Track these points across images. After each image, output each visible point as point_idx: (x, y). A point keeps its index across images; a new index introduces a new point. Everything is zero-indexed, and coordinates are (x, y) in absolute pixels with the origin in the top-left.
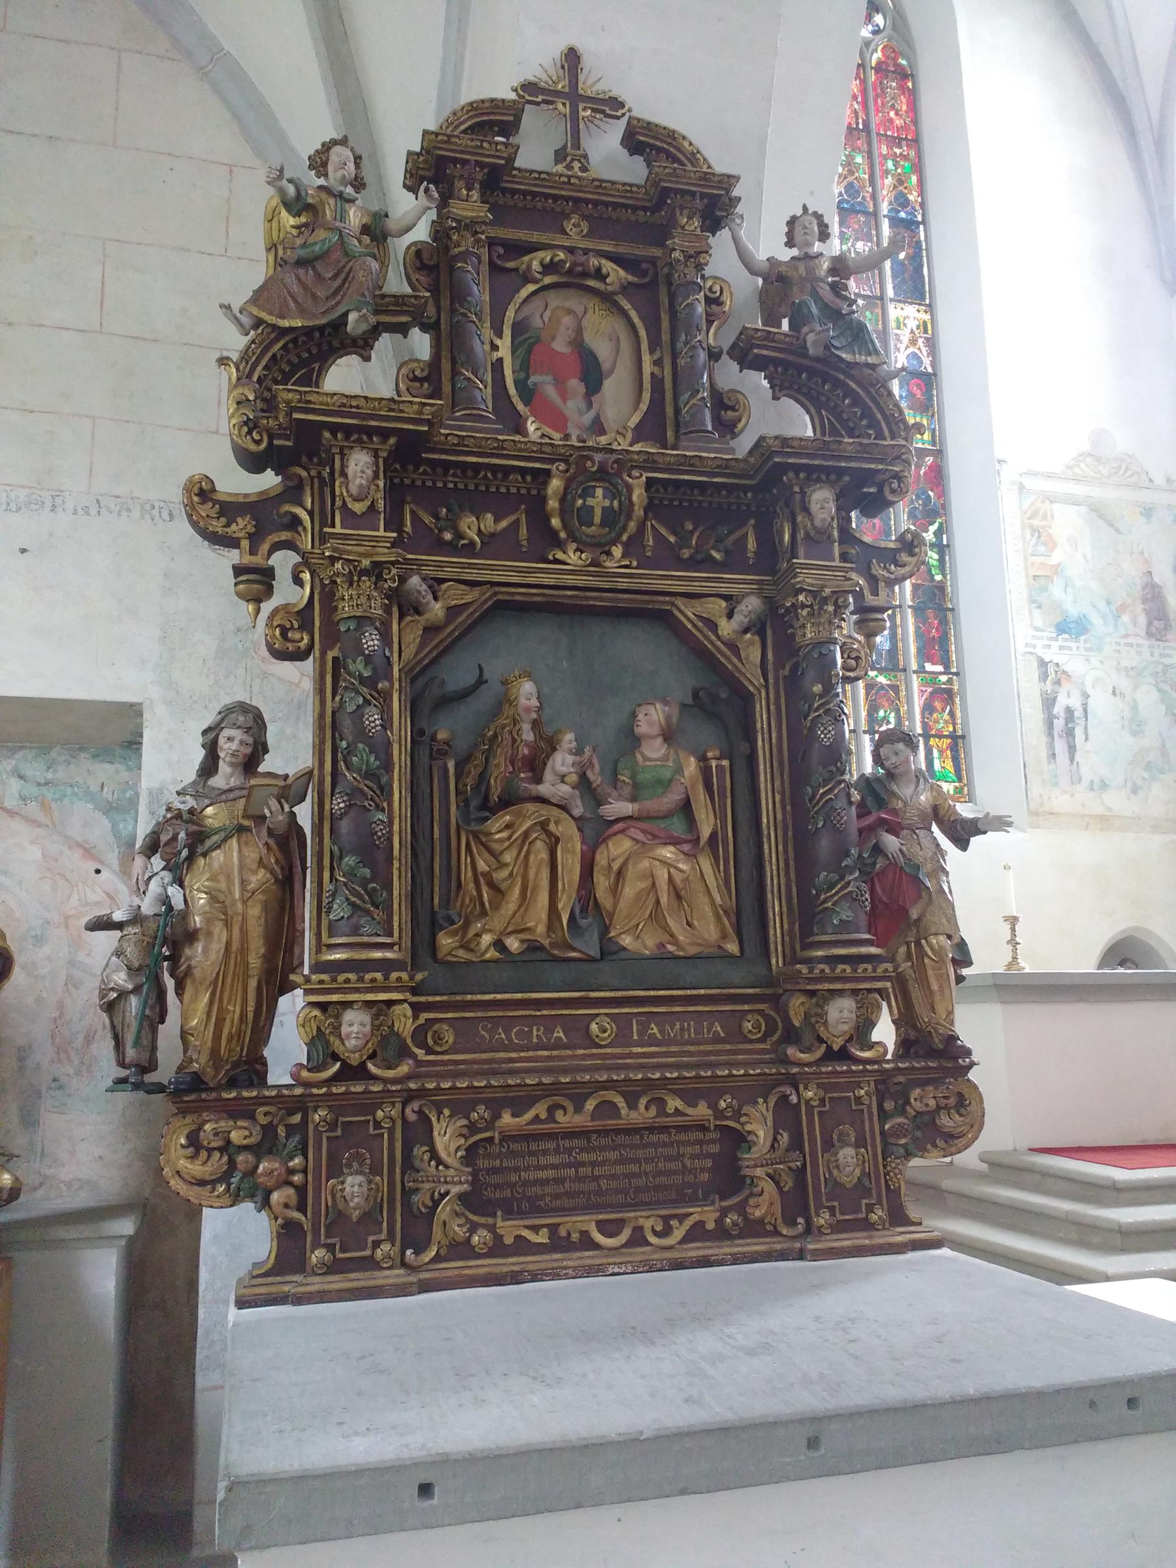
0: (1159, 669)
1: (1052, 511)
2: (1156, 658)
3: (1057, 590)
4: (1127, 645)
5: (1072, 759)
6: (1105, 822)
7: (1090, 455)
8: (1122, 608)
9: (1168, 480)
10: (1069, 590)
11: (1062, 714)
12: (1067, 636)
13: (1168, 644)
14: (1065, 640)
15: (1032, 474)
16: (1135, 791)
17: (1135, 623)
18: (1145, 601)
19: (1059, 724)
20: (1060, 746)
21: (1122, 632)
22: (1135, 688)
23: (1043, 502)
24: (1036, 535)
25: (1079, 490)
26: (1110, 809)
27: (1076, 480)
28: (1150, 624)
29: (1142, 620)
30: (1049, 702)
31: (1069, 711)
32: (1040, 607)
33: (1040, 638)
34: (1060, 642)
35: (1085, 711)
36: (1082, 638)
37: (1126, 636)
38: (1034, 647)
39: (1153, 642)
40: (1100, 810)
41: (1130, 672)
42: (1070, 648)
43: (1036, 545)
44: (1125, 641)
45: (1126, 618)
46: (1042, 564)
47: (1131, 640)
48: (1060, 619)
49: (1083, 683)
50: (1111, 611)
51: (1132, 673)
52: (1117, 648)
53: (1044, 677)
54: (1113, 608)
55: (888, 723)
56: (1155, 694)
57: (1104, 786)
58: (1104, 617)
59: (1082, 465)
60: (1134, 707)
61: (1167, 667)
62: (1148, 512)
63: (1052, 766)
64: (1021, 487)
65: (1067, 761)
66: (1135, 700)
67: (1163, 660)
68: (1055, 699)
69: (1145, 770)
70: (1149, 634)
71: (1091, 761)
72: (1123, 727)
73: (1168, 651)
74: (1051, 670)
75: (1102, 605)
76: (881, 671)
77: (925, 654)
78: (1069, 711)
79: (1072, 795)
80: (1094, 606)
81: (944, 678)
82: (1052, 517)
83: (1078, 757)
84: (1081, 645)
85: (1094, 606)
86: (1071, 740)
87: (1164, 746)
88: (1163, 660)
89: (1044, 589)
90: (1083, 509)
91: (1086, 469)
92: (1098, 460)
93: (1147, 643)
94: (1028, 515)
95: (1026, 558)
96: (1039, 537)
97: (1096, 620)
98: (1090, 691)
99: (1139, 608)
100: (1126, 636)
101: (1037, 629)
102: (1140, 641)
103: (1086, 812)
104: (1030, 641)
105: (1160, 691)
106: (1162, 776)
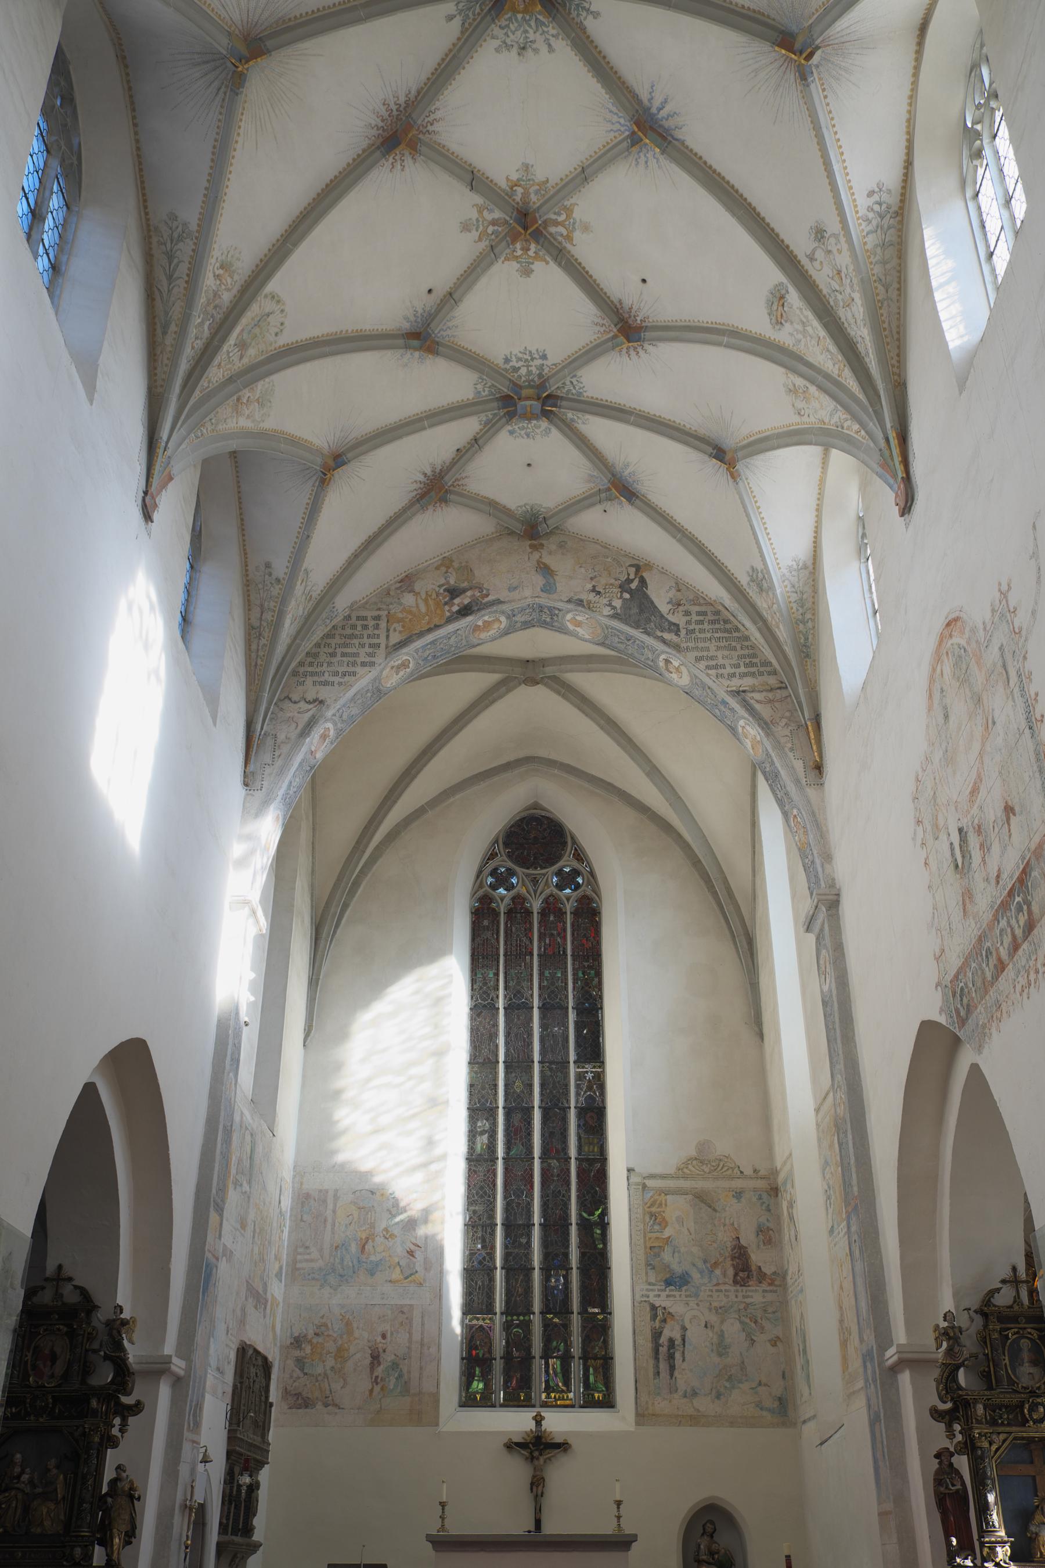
0: (742, 1306)
1: (666, 1201)
2: (740, 1299)
3: (667, 1256)
4: (717, 1291)
5: (672, 1375)
6: (695, 1420)
7: (696, 1159)
8: (716, 1264)
9: (755, 1171)
10: (676, 1254)
11: (666, 1343)
12: (673, 1288)
13: (749, 1288)
14: (671, 1290)
15: (652, 1176)
16: (718, 1396)
17: (724, 1275)
18: (733, 1258)
19: (663, 1350)
20: (663, 1366)
21: (715, 1281)
22: (722, 1322)
23: (660, 1195)
24: (653, 1218)
26: (698, 1411)
27: (685, 1177)
28: (736, 1275)
29: (731, 1272)
30: (657, 1335)
31: (671, 1341)
32: (654, 1268)
33: (652, 1290)
34: (667, 1293)
35: (684, 1340)
36: (685, 1288)
37: (718, 1284)
38: (648, 1297)
39: (738, 1287)
41: (722, 1311)
42: (674, 1296)
43: (652, 1226)
44: (716, 1288)
45: (718, 1272)
46: (657, 1238)
47: (722, 1287)
48: (668, 1276)
49: (683, 1320)
50: (707, 1268)
51: (720, 1311)
52: (710, 1293)
53: (654, 1317)
54: (708, 1265)
55: (559, 1350)
56: (737, 1326)
57: (695, 1394)
58: (701, 1272)
59: (690, 1167)
60: (721, 1335)
62: (738, 1195)
63: (657, 1380)
64: (644, 1186)
65: (669, 1377)
66: (722, 1331)
67: (746, 1300)
68: (661, 1333)
69: (727, 1381)
70: (735, 1282)
71: (685, 1376)
72: (712, 1350)
73: (750, 1294)
74: (660, 1312)
75: (700, 1264)
76: (556, 1315)
77: (585, 1302)
78: (671, 1341)
79: (670, 1401)
80: (694, 1265)
81: (600, 1317)
82: (666, 1205)
83: (676, 1373)
84: (683, 1293)
85: (694, 1265)
86: (671, 1361)
87: (743, 1363)
88: (746, 1300)
89: (657, 1255)
90: (690, 1197)
91: (693, 1169)
93: (733, 1288)
94: (648, 1205)
95: (645, 1237)
96: (656, 1219)
97: (695, 1275)
98: (688, 1325)
99: (729, 1262)
100: (718, 1284)
101: (650, 1284)
102: (727, 1287)
103: (680, 1413)
104: (644, 1292)
105: (741, 1322)
106: (740, 1385)
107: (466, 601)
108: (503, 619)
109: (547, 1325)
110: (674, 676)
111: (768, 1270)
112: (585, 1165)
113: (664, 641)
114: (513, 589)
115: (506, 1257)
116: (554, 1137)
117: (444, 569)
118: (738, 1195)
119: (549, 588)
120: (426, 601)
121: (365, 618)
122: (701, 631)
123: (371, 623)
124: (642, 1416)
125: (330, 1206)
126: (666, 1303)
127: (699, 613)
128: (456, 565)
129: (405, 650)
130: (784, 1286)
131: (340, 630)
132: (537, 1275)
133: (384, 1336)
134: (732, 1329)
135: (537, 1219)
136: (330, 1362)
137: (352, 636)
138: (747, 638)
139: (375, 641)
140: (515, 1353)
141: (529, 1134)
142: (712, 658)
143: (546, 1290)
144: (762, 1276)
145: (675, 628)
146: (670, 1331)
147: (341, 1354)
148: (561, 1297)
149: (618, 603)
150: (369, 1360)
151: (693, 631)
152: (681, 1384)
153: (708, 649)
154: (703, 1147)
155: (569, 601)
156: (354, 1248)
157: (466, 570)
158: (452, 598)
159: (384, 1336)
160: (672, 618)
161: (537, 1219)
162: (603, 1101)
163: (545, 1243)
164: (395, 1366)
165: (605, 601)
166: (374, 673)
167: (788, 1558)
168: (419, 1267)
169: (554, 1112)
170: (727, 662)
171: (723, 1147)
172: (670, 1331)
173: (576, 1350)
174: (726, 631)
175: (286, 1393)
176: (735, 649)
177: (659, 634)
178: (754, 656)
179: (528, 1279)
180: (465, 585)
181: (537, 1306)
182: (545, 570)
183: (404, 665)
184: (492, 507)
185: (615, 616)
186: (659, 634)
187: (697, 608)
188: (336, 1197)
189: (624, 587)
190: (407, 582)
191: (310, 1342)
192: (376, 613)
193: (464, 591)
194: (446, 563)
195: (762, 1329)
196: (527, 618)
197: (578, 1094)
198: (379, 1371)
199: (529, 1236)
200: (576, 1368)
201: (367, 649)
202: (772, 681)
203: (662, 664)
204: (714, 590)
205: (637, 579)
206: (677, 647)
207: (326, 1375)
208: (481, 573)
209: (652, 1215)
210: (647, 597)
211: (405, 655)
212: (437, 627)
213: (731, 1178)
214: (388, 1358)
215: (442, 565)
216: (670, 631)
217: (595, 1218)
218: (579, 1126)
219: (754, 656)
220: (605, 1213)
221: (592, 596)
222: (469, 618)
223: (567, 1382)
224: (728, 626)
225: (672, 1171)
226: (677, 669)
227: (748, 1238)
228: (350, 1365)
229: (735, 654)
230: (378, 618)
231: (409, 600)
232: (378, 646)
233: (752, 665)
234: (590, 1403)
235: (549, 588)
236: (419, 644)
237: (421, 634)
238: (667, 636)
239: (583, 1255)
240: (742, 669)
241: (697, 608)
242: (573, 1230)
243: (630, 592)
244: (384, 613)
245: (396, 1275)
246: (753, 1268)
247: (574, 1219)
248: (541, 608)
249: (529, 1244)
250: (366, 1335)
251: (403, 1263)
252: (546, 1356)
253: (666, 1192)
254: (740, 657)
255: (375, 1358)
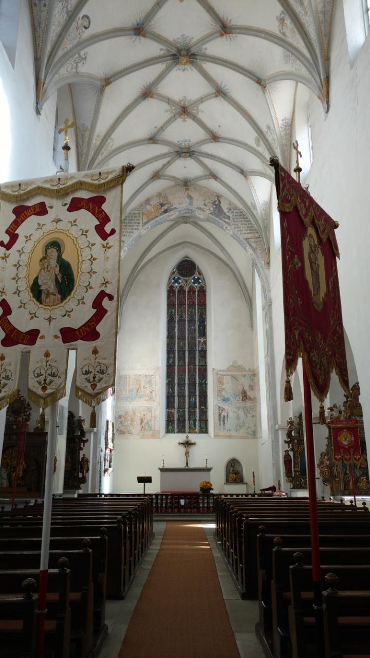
3: (223, 393)
6: (230, 437)
8: (237, 395)
15: (219, 371)
16: (237, 431)
18: (242, 393)
19: (222, 419)
20: (222, 423)
25: (228, 373)
27: (229, 371)
29: (241, 397)
30: (220, 415)
31: (224, 416)
40: (229, 435)
41: (238, 408)
45: (238, 397)
53: (219, 410)
57: (230, 430)
58: (233, 397)
60: (238, 415)
61: (245, 407)
62: (244, 376)
64: (217, 374)
70: (243, 400)
71: (227, 426)
75: (233, 395)
78: (224, 416)
83: (225, 425)
90: (230, 377)
92: (234, 367)
97: (231, 398)
98: (229, 412)
99: (241, 395)
105: (244, 411)
107: (166, 208)
108: (177, 213)
109: (189, 412)
110: (228, 232)
111: (252, 397)
112: (201, 367)
113: (225, 222)
114: (180, 204)
115: (178, 393)
116: (192, 358)
117: (159, 197)
118: (244, 376)
119: (191, 204)
120: (154, 207)
121: (135, 214)
122: (237, 219)
123: (137, 215)
124: (216, 436)
125: (128, 380)
126: (223, 406)
127: (236, 213)
128: (162, 195)
129: (148, 224)
130: (256, 401)
131: (128, 218)
132: (187, 398)
133: (144, 415)
134: (241, 413)
135: (187, 382)
136: (129, 422)
137: (132, 220)
138: (250, 221)
139: (139, 221)
140: (181, 419)
141: (185, 358)
142: (239, 228)
143: (189, 402)
144: (250, 399)
145: (229, 217)
146: (224, 414)
147: (132, 420)
148: (194, 404)
149: (212, 209)
150: (140, 422)
151: (234, 219)
152: (226, 428)
153: (238, 225)
154: (234, 362)
155: (197, 208)
156: (135, 391)
157: (166, 197)
158: (162, 207)
159: (144, 415)
160: (228, 214)
161: (187, 382)
162: (206, 348)
163: (189, 389)
164: (147, 423)
165: (208, 208)
166: (139, 231)
167: (253, 472)
168: (154, 396)
169: (192, 352)
170: (244, 229)
171: (240, 362)
172: (224, 414)
173: (198, 418)
174: (244, 218)
175: (117, 430)
176: (246, 225)
177: (224, 219)
178: (252, 227)
179: (184, 399)
180: (165, 202)
181: (187, 406)
182: (190, 197)
183: (148, 228)
184: (174, 178)
185: (211, 213)
186: (224, 219)
187: (236, 211)
188: (129, 377)
189: (214, 203)
190: (148, 201)
191: (124, 417)
192: (138, 212)
193: (165, 205)
194: (159, 195)
195: (250, 413)
196: (184, 212)
197: (199, 346)
198: (143, 424)
199: (185, 387)
200: (198, 423)
201: (136, 224)
202: (257, 235)
203: (225, 228)
204: (240, 206)
205: (217, 202)
206: (229, 224)
207: (128, 426)
208: (170, 198)
209: (219, 381)
210: (220, 207)
211: (148, 225)
212: (157, 217)
213: (242, 371)
214: (145, 421)
215: (158, 195)
216: (227, 218)
217: (203, 382)
218: (199, 356)
219: (252, 227)
220: (206, 380)
221: (204, 207)
222: (167, 214)
223: (195, 426)
224: (245, 217)
225: (225, 369)
226: (229, 230)
227: (247, 388)
228: (135, 423)
229: (246, 226)
230: (139, 214)
231: (148, 207)
232: (139, 223)
233: (250, 230)
234: (201, 432)
235: (191, 204)
236: (152, 222)
237: (152, 219)
238: (226, 220)
239: (200, 392)
240: (248, 231)
241: (236, 211)
242: (197, 385)
243: (215, 205)
244: (141, 212)
245: (147, 398)
246: (248, 396)
247: (197, 382)
248: (188, 209)
249: (184, 389)
250: (139, 415)
251: (149, 395)
252: (189, 420)
253: (223, 375)
254: (248, 227)
255: (142, 421)
